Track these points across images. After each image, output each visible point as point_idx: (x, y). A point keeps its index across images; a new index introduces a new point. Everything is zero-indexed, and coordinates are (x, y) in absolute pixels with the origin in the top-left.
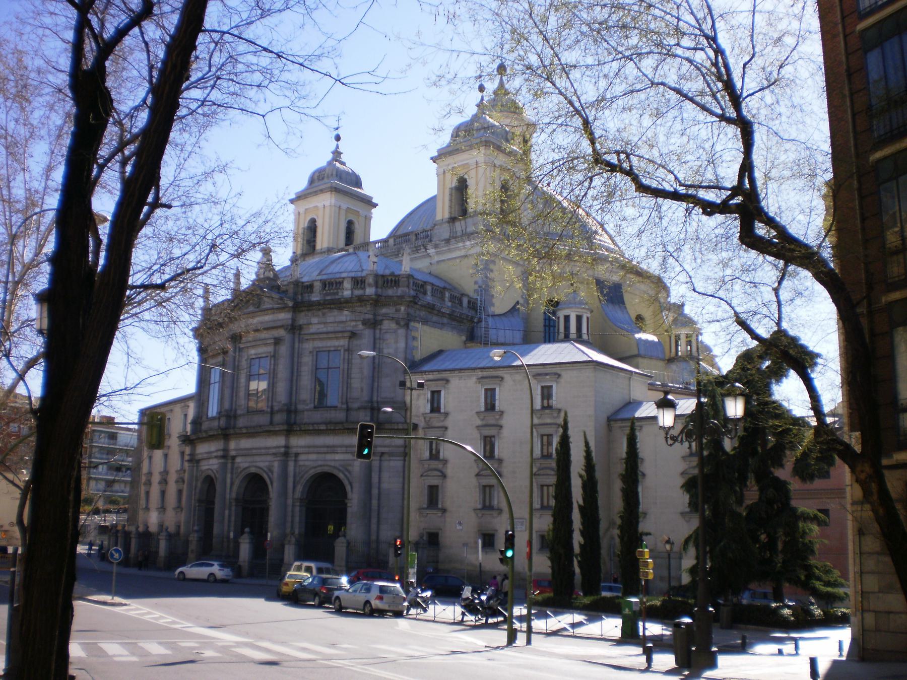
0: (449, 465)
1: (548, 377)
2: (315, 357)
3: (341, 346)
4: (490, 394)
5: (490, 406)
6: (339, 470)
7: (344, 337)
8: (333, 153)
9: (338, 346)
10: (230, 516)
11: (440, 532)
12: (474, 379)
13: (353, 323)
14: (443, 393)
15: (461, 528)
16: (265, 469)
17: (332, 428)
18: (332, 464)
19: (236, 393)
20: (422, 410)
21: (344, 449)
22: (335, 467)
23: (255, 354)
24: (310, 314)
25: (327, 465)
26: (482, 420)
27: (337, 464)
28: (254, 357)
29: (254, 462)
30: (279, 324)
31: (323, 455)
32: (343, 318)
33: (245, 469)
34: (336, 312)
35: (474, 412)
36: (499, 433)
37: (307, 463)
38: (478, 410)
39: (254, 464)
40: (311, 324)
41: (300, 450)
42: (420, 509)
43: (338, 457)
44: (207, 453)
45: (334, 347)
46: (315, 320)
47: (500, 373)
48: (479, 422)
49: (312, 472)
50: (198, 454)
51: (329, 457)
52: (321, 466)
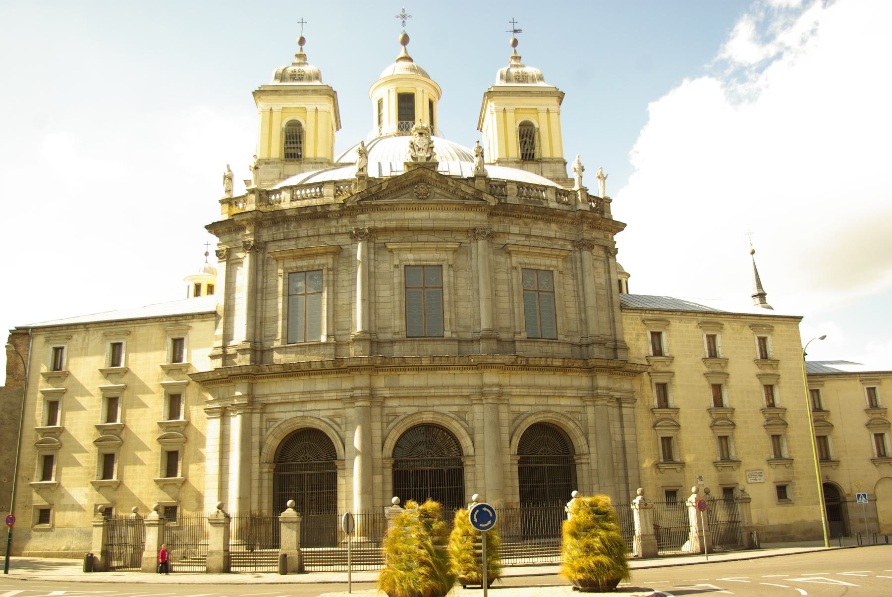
0: (681, 415)
1: (764, 328)
2: (521, 276)
3: (555, 267)
4: (712, 339)
5: (713, 354)
6: (570, 419)
7: (557, 256)
9: (551, 266)
10: (384, 483)
11: (680, 489)
12: (695, 324)
13: (560, 242)
14: (664, 336)
15: (702, 483)
16: (453, 416)
18: (558, 409)
19: (375, 309)
20: (644, 352)
21: (573, 393)
22: (562, 415)
23: (415, 260)
24: (507, 220)
25: (552, 412)
26: (708, 367)
27: (564, 410)
28: (412, 263)
29: (428, 406)
30: (466, 225)
31: (545, 399)
32: (552, 235)
34: (541, 225)
35: (700, 358)
36: (726, 382)
37: (523, 409)
39: (430, 409)
41: (515, 391)
42: (657, 465)
43: (563, 402)
44: (303, 393)
45: (546, 266)
46: (515, 229)
47: (719, 320)
48: (705, 369)
49: (532, 420)
50: (267, 396)
51: (551, 401)
52: (544, 412)
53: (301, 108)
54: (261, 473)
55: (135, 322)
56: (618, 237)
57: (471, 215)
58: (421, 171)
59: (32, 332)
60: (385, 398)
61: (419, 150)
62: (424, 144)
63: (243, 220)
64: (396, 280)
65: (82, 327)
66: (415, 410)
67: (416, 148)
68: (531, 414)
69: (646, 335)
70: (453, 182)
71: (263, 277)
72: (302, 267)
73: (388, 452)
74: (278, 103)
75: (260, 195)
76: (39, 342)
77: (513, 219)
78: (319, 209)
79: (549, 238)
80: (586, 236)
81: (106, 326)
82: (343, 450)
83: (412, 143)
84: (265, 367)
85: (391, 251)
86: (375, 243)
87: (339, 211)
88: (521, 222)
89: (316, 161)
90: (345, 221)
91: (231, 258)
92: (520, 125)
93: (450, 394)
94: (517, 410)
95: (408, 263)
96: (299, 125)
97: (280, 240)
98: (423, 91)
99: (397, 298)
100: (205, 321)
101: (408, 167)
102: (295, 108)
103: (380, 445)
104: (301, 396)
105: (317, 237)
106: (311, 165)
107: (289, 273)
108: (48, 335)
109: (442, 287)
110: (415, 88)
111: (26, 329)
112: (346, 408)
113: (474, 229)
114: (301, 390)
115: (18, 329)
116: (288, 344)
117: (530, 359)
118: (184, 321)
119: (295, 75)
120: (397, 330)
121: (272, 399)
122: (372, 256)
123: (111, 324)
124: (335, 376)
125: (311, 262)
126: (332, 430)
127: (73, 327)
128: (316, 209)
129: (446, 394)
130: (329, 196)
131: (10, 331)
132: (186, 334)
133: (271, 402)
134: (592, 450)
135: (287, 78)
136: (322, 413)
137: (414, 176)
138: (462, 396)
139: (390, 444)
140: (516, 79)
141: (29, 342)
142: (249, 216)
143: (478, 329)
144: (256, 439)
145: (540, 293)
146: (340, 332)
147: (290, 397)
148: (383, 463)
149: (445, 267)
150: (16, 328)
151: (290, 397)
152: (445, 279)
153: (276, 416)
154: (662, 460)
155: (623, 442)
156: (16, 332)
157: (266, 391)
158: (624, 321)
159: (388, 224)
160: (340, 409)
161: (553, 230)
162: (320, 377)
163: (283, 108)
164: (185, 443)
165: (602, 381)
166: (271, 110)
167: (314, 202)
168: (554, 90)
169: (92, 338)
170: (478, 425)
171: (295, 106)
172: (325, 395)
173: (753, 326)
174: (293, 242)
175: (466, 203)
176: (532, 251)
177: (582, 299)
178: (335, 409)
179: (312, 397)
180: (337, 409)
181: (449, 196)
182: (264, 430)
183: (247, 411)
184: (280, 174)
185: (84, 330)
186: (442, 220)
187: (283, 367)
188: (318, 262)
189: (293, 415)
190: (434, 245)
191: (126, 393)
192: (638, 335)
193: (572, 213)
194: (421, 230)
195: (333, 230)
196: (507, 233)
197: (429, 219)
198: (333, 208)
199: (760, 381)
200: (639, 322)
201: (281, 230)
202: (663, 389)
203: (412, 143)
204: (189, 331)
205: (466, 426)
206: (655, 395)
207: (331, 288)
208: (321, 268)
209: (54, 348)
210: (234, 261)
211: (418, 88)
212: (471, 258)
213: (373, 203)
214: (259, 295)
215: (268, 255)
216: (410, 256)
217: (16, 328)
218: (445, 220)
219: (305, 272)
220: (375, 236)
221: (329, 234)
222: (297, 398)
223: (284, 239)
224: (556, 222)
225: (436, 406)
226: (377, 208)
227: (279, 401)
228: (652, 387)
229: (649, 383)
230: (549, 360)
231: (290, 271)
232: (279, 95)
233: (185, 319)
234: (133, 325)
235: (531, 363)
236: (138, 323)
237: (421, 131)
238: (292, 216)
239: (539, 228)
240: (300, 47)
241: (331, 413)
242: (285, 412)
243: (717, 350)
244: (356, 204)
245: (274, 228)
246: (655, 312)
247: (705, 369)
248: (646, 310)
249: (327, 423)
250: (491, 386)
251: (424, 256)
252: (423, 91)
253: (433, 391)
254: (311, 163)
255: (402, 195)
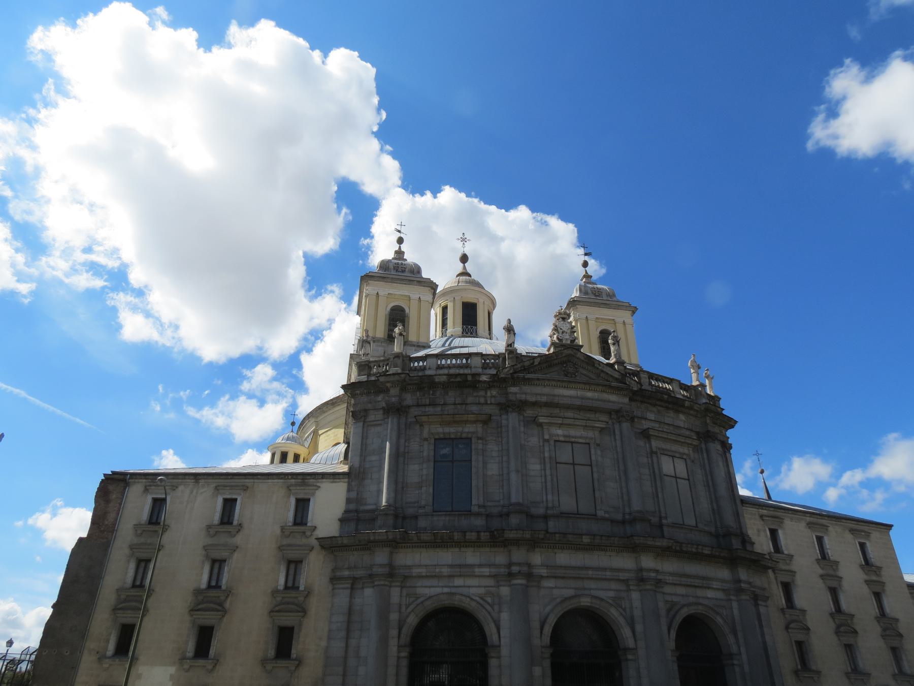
1: (863, 534)
5: (824, 556)
6: (717, 613)
8: (396, 252)
9: (684, 454)
14: (780, 532)
16: (611, 602)
17: (717, 554)
23: (565, 436)
25: (700, 604)
26: (822, 569)
28: (562, 439)
29: (585, 589)
32: (682, 424)
33: (565, 600)
34: (671, 414)
37: (675, 599)
38: (816, 557)
40: (646, 419)
41: (670, 579)
43: (710, 594)
44: (451, 566)
45: (680, 453)
46: (651, 416)
48: (821, 572)
49: (685, 612)
50: (410, 567)
51: (700, 593)
53: (405, 295)
54: (399, 658)
55: (255, 477)
56: (729, 433)
57: (613, 398)
58: (570, 352)
59: (129, 479)
60: (542, 577)
61: (563, 333)
62: (567, 328)
63: (388, 382)
64: (547, 455)
65: (192, 477)
66: (571, 592)
67: (561, 331)
68: (684, 606)
69: (765, 531)
70: (599, 365)
71: (405, 441)
72: (449, 433)
73: (547, 640)
74: (384, 289)
75: (403, 360)
76: (135, 491)
77: (648, 405)
78: (469, 378)
79: (678, 427)
80: (710, 428)
81: (220, 479)
82: (497, 636)
83: (556, 326)
84: (413, 535)
85: (540, 425)
86: (524, 417)
87: (489, 382)
88: (655, 409)
89: (419, 344)
90: (494, 392)
91: (367, 420)
92: (600, 333)
93: (608, 577)
94: (670, 600)
95: (557, 438)
96: (403, 310)
97: (425, 406)
98: (484, 302)
99: (548, 472)
100: (336, 482)
101: (555, 348)
102: (400, 295)
103: (539, 630)
104: (449, 570)
105: (464, 406)
106: (414, 348)
107: (435, 439)
108: (148, 484)
109: (591, 465)
110: (478, 299)
111: (124, 474)
112: (501, 586)
113: (618, 412)
114: (450, 563)
115: (114, 473)
116: (433, 512)
117: (684, 545)
118: (311, 480)
119: (398, 267)
120: (550, 505)
121: (416, 571)
122: (522, 429)
123: (226, 477)
124: (487, 549)
125: (460, 429)
126: (484, 611)
127: (180, 477)
128: (467, 377)
129: (604, 577)
130: (476, 367)
131: (105, 475)
132: (313, 494)
133: (414, 574)
134: (743, 649)
135: (390, 269)
136: (473, 591)
137: (564, 355)
138: (619, 580)
139: (548, 630)
140: (593, 293)
141: (125, 489)
142: (397, 378)
143: (627, 510)
144: (394, 617)
145: (678, 480)
146: (489, 504)
147: (437, 570)
148: (542, 652)
149: (592, 446)
150: (112, 472)
151: (437, 570)
152: (593, 458)
153: (420, 591)
154: (799, 667)
155: (764, 643)
156: (111, 477)
157: (409, 563)
158: (745, 515)
159: (539, 398)
160: (491, 587)
161: (682, 420)
162: (472, 549)
163: (389, 294)
164: (303, 617)
165: (743, 574)
166: (378, 293)
167: (462, 371)
168: (628, 305)
169: (202, 491)
170: (637, 613)
171: (398, 293)
172: (477, 570)
173: (852, 531)
174: (439, 409)
175: (612, 385)
176: (669, 437)
177: (712, 489)
178: (488, 587)
179: (464, 570)
180: (488, 587)
181: (595, 378)
182: (403, 609)
183: (387, 583)
184: (385, 352)
185: (193, 481)
186: (589, 399)
187: (434, 535)
188: (466, 430)
189: (439, 590)
190: (583, 423)
191: (236, 555)
192: (758, 531)
193: (698, 406)
194: (568, 407)
195: (482, 400)
196: (644, 418)
197: (577, 397)
198: (484, 378)
199: (869, 588)
200: (757, 517)
201: (426, 395)
202: (787, 588)
203: (556, 326)
204: (317, 492)
205: (624, 613)
206: (782, 594)
207: (481, 458)
208: (470, 436)
209: (153, 498)
210: (372, 423)
211: (479, 299)
212: (615, 440)
213: (526, 377)
214: (401, 459)
215: (410, 420)
216: (560, 432)
217: (112, 472)
218: (592, 399)
219: (452, 439)
220: (525, 409)
221: (476, 404)
222: (445, 571)
223: (429, 405)
224: (684, 413)
225: (593, 589)
226: (528, 381)
227: (424, 574)
228: (778, 586)
229: (775, 581)
230: (700, 547)
231: (437, 437)
232: (386, 282)
233: (313, 479)
234: (252, 481)
235: (684, 549)
236: (258, 479)
237: (564, 316)
238: (440, 383)
239: (670, 417)
240: (399, 245)
241: (481, 591)
242: (430, 587)
243: (826, 551)
244: (510, 376)
245: (418, 393)
246: (771, 509)
247: (821, 572)
248: (763, 506)
249: (478, 603)
250: (649, 570)
251: (573, 432)
252: (484, 302)
253: (590, 572)
254: (414, 346)
255: (550, 372)
